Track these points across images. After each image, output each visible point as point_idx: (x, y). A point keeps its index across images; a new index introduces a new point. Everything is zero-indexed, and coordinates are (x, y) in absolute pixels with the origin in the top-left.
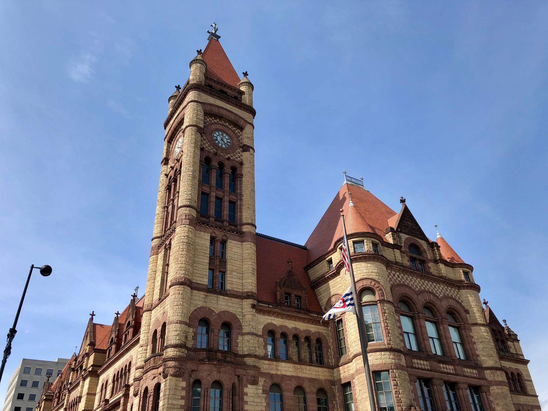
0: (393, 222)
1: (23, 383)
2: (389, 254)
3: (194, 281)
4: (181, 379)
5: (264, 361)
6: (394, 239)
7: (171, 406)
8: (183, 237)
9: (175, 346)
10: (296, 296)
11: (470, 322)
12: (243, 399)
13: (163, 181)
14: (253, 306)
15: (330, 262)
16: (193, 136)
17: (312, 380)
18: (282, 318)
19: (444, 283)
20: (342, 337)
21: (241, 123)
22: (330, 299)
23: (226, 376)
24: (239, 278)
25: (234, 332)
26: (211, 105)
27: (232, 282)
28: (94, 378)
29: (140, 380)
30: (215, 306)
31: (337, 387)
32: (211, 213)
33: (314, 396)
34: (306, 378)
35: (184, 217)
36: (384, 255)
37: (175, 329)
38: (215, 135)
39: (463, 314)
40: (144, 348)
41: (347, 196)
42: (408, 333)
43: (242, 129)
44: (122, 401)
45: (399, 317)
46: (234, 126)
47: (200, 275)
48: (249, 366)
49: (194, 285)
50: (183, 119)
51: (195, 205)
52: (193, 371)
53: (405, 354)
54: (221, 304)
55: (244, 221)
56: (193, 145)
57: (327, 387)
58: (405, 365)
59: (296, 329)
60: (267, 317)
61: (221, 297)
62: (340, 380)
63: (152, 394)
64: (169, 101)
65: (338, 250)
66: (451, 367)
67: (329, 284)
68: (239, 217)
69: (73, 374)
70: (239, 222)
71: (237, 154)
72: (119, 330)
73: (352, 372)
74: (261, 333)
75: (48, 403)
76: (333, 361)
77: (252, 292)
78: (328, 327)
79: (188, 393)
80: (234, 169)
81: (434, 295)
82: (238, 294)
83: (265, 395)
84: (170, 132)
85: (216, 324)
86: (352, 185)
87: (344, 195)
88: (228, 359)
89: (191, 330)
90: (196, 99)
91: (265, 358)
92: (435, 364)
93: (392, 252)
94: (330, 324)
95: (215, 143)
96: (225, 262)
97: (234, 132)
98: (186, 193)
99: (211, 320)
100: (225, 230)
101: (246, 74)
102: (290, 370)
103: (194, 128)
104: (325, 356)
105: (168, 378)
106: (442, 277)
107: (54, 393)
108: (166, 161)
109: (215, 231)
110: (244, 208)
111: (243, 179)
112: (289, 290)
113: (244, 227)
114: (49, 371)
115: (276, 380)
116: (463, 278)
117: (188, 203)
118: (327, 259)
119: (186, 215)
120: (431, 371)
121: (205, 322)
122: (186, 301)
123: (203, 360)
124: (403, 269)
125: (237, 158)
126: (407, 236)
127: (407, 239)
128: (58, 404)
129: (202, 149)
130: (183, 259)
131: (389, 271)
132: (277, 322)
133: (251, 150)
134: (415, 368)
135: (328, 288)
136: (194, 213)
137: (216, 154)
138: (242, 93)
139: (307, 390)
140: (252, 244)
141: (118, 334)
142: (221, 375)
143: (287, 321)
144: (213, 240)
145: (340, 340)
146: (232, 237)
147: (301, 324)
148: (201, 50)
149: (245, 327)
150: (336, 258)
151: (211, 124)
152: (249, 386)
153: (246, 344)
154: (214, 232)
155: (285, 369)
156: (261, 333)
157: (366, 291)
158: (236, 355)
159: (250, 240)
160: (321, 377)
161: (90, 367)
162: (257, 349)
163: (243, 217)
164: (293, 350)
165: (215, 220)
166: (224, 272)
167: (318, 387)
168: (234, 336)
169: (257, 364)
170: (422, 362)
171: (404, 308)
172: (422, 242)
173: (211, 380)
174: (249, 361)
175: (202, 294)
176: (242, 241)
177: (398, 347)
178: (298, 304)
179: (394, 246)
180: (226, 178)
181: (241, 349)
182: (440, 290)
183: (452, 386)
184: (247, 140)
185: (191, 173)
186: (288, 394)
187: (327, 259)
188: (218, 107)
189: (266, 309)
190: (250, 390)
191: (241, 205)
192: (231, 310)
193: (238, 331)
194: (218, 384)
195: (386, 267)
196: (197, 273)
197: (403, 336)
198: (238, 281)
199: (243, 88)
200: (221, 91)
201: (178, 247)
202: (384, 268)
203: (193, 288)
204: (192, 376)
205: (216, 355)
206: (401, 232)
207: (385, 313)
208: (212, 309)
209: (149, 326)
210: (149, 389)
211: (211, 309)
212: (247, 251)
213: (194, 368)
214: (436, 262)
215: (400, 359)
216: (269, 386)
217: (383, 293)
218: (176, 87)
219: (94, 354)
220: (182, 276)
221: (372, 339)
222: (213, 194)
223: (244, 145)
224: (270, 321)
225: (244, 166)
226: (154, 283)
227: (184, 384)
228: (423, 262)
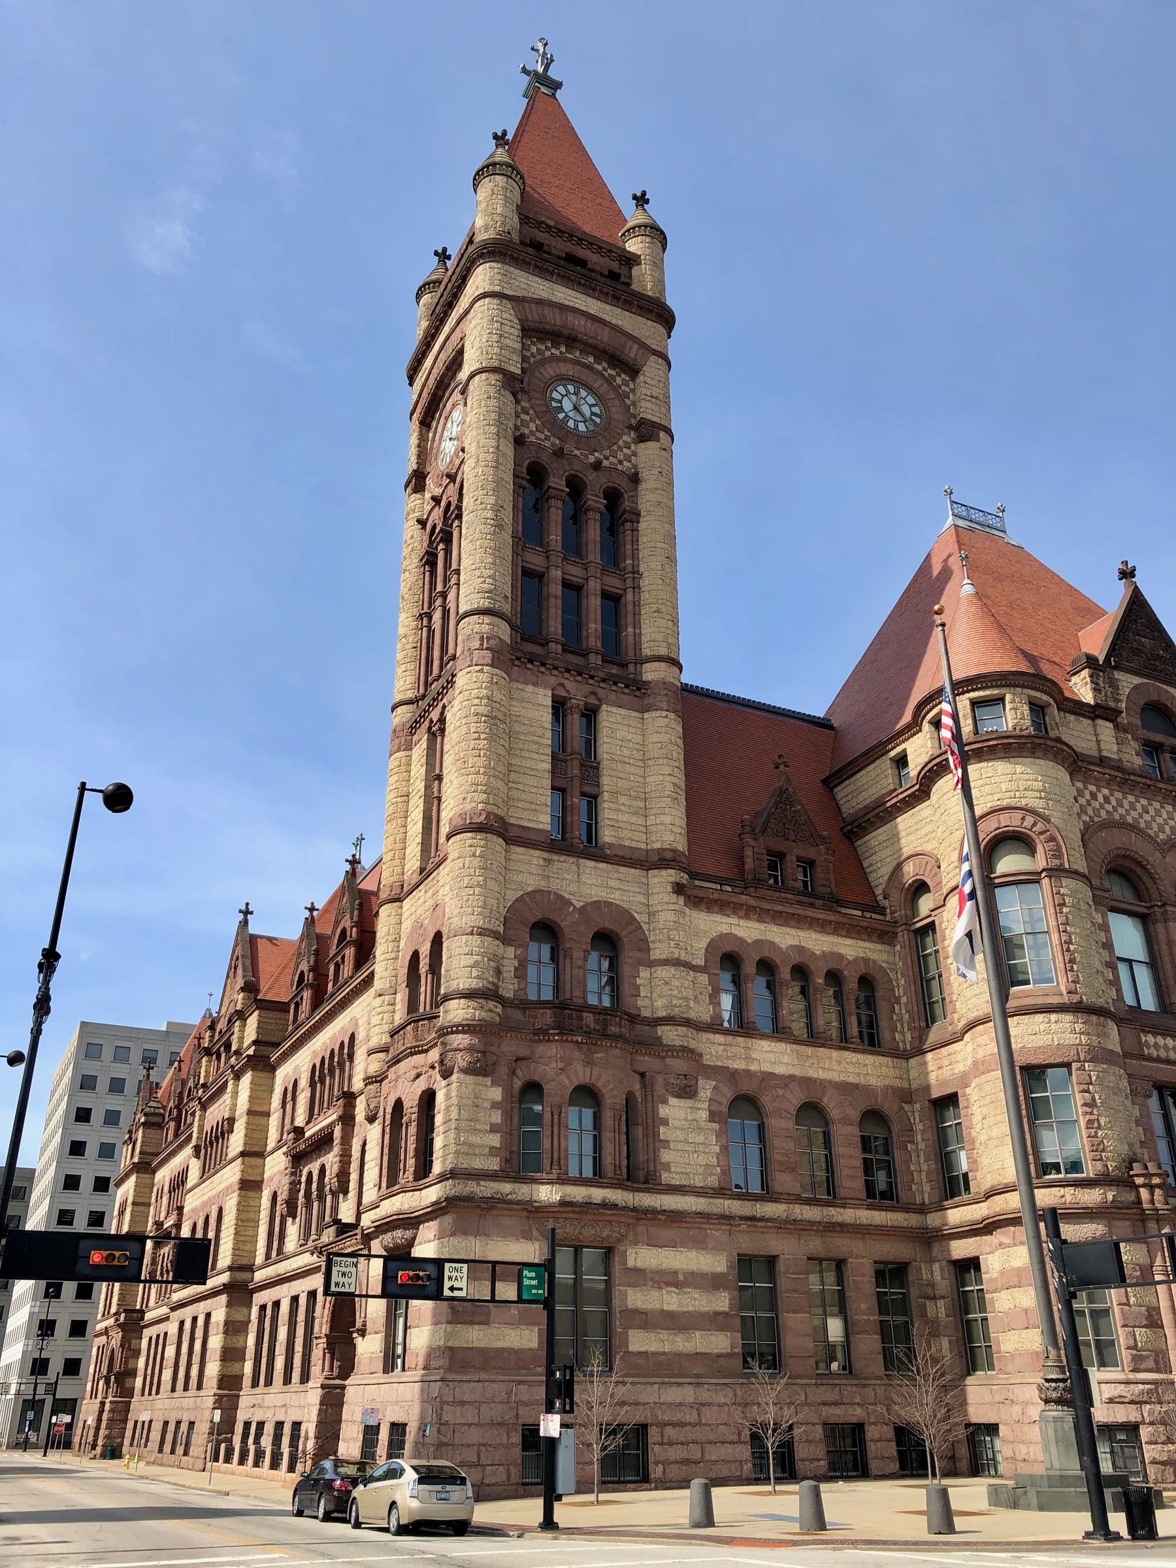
0: (1096, 640)
1: (86, 1083)
2: (1080, 735)
3: (513, 821)
4: (488, 1081)
5: (711, 1036)
6: (1096, 690)
7: (465, 1149)
8: (477, 701)
9: (469, 995)
12: (656, 1134)
13: (412, 541)
14: (679, 889)
15: (902, 761)
16: (493, 402)
17: (846, 1088)
18: (760, 920)
20: (933, 972)
21: (632, 355)
22: (899, 867)
23: (610, 1074)
24: (636, 813)
25: (628, 956)
26: (540, 302)
27: (618, 824)
28: (262, 1075)
29: (381, 1081)
30: (573, 888)
31: (917, 1106)
32: (552, 629)
33: (854, 1131)
34: (830, 1081)
35: (477, 644)
36: (1065, 738)
37: (466, 950)
38: (555, 395)
40: (387, 998)
41: (955, 563)
42: (1130, 962)
43: (633, 371)
45: (1104, 916)
46: (612, 366)
47: (527, 805)
48: (671, 1049)
49: (512, 833)
50: (460, 352)
51: (506, 608)
52: (518, 1059)
53: (1120, 1021)
54: (587, 884)
55: (647, 652)
56: (493, 429)
57: (889, 1107)
58: (1118, 1049)
59: (800, 949)
60: (718, 918)
62: (928, 1088)
63: (414, 1116)
64: (418, 297)
65: (926, 727)
67: (896, 825)
68: (631, 639)
69: (210, 1061)
70: (631, 653)
71: (620, 449)
72: (317, 950)
73: (960, 1068)
74: (700, 962)
75: (152, 1132)
76: (908, 1037)
77: (675, 851)
78: (894, 946)
79: (507, 1115)
80: (613, 497)
82: (636, 856)
83: (716, 1126)
84: (425, 394)
85: (577, 937)
86: (971, 530)
87: (946, 561)
88: (613, 1029)
89: (510, 952)
90: (497, 289)
91: (714, 1027)
93: (1090, 729)
94: (900, 938)
95: (555, 418)
96: (597, 768)
97: (610, 381)
98: (478, 573)
99: (563, 924)
100: (592, 677)
101: (641, 200)
102: (786, 1059)
103: (493, 378)
104: (883, 1023)
105: (454, 1077)
107: (164, 1108)
108: (418, 481)
109: (566, 682)
111: (642, 526)
112: (778, 845)
113: (647, 667)
114: (147, 1054)
115: (747, 1087)
117: (486, 604)
118: (892, 754)
119: (482, 639)
121: (546, 930)
122: (493, 874)
123: (545, 1032)
124: (1121, 777)
125: (621, 462)
126: (1137, 680)
127: (1136, 687)
128: (176, 1135)
129: (519, 441)
130: (481, 762)
131: (1080, 785)
132: (748, 930)
133: (662, 435)
134: (1150, 1059)
135: (895, 837)
136: (504, 632)
137: (559, 453)
138: (632, 260)
140: (672, 716)
141: (316, 961)
142: (596, 1072)
143: (775, 928)
144: (559, 707)
145: (928, 981)
146: (613, 697)
147: (815, 936)
148: (505, 133)
149: (658, 945)
150: (919, 749)
151: (544, 361)
152: (673, 1101)
153: (660, 991)
154: (562, 685)
155: (772, 1057)
156: (700, 962)
157: (1007, 845)
158: (634, 1019)
159: (665, 705)
160: (873, 1081)
161: (249, 1048)
162: (692, 1004)
163: (645, 639)
164: (792, 1007)
165: (563, 650)
166: (595, 797)
167: (864, 1105)
168: (626, 970)
169: (693, 1044)
171: (1120, 891)
173: (568, 1083)
174: (671, 1035)
176: (643, 710)
177: (1100, 1002)
178: (805, 883)
180: (591, 523)
181: (647, 1002)
184: (648, 405)
185: (490, 514)
186: (781, 1125)
187: (892, 754)
188: (562, 308)
189: (716, 896)
190: (674, 1110)
191: (637, 604)
192: (616, 898)
193: (638, 955)
194: (587, 1094)
195: (1071, 775)
196: (519, 800)
197: (1115, 969)
198: (633, 819)
199: (634, 246)
200: (571, 258)
201: (464, 729)
202: (1063, 775)
203: (509, 841)
204: (519, 1072)
205: (580, 1018)
206: (1116, 668)
207: (1063, 904)
208: (567, 896)
209: (397, 940)
210: (407, 1104)
211: (562, 898)
213: (523, 1052)
215: (1105, 1035)
216: (726, 1102)
217: (1059, 849)
218: (436, 253)
219: (256, 1013)
220: (480, 806)
221: (1021, 977)
222: (556, 574)
223: (643, 422)
224: (725, 929)
226: (405, 826)
227: (496, 1094)
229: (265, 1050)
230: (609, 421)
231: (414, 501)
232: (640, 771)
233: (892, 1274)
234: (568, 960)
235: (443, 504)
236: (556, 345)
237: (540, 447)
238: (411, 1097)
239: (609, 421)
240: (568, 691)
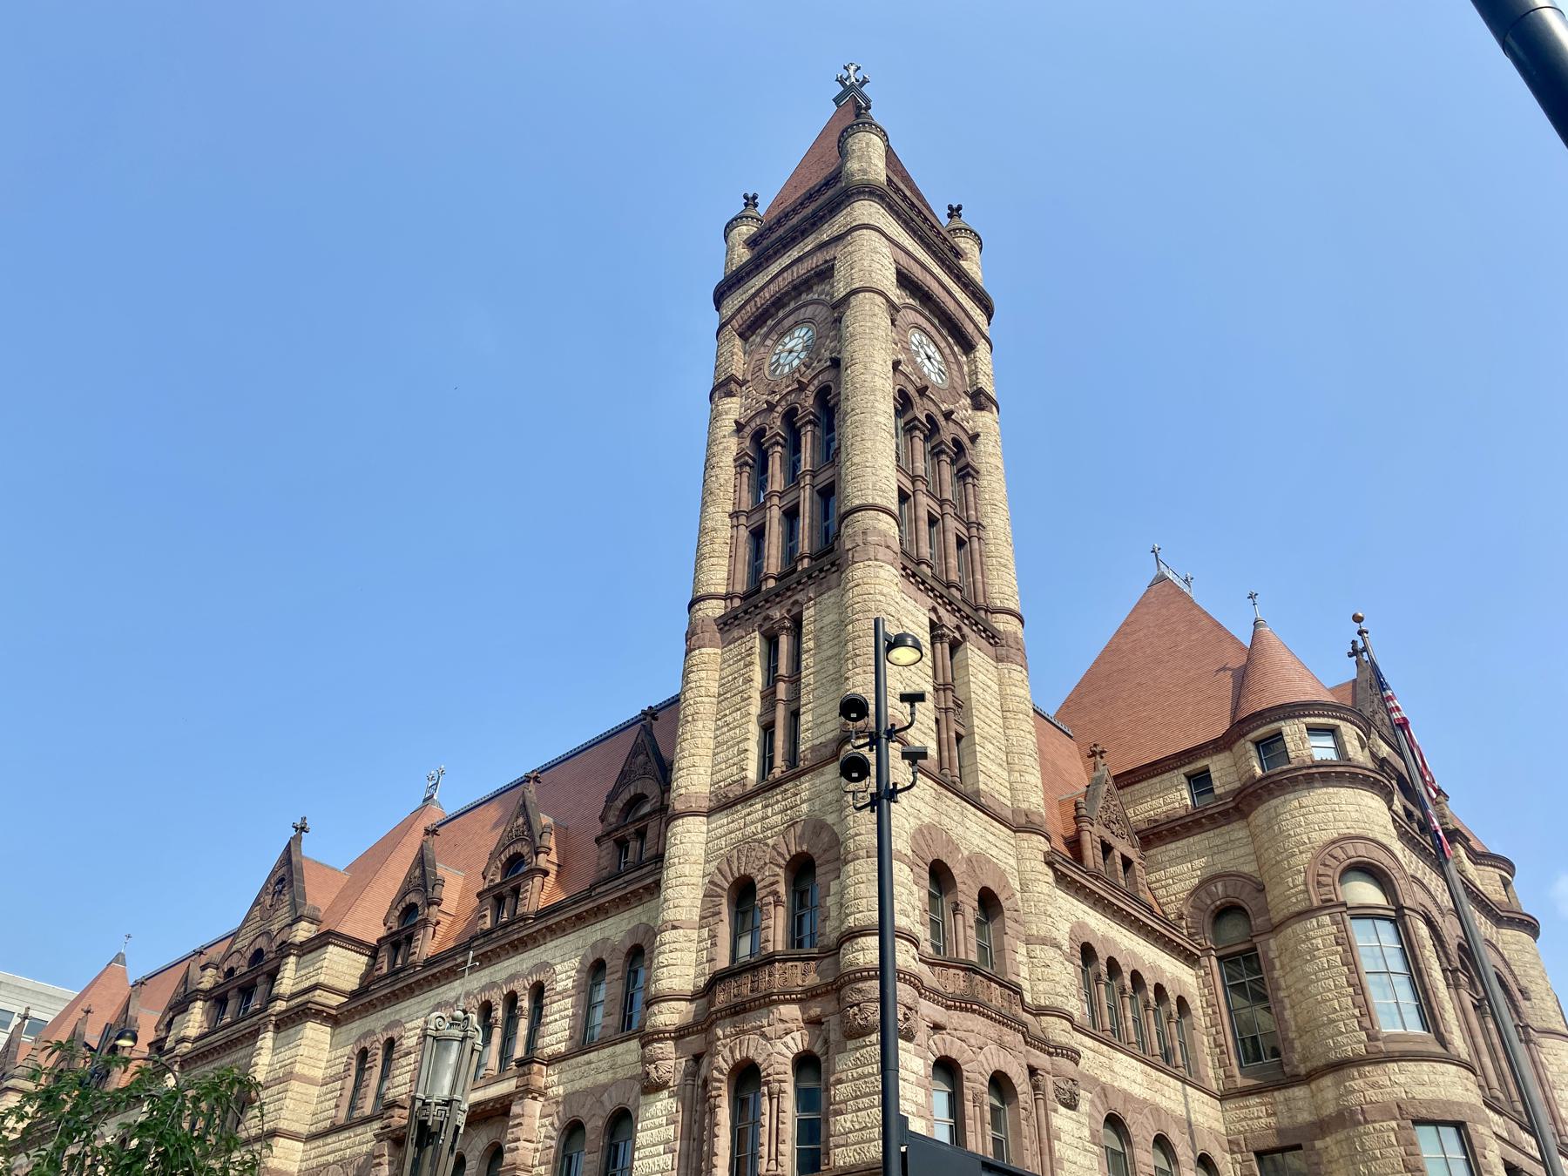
10: (1123, 857)
59: (1133, 955)
64: (729, 227)
68: (979, 585)
70: (981, 600)
101: (954, 212)
109: (941, 611)
115: (1119, 1107)
129: (896, 365)
152: (1062, 1109)
174: (1058, 1030)
198: (1000, 771)
218: (746, 197)
232: (1000, 721)
234: (959, 917)
240: (939, 618)
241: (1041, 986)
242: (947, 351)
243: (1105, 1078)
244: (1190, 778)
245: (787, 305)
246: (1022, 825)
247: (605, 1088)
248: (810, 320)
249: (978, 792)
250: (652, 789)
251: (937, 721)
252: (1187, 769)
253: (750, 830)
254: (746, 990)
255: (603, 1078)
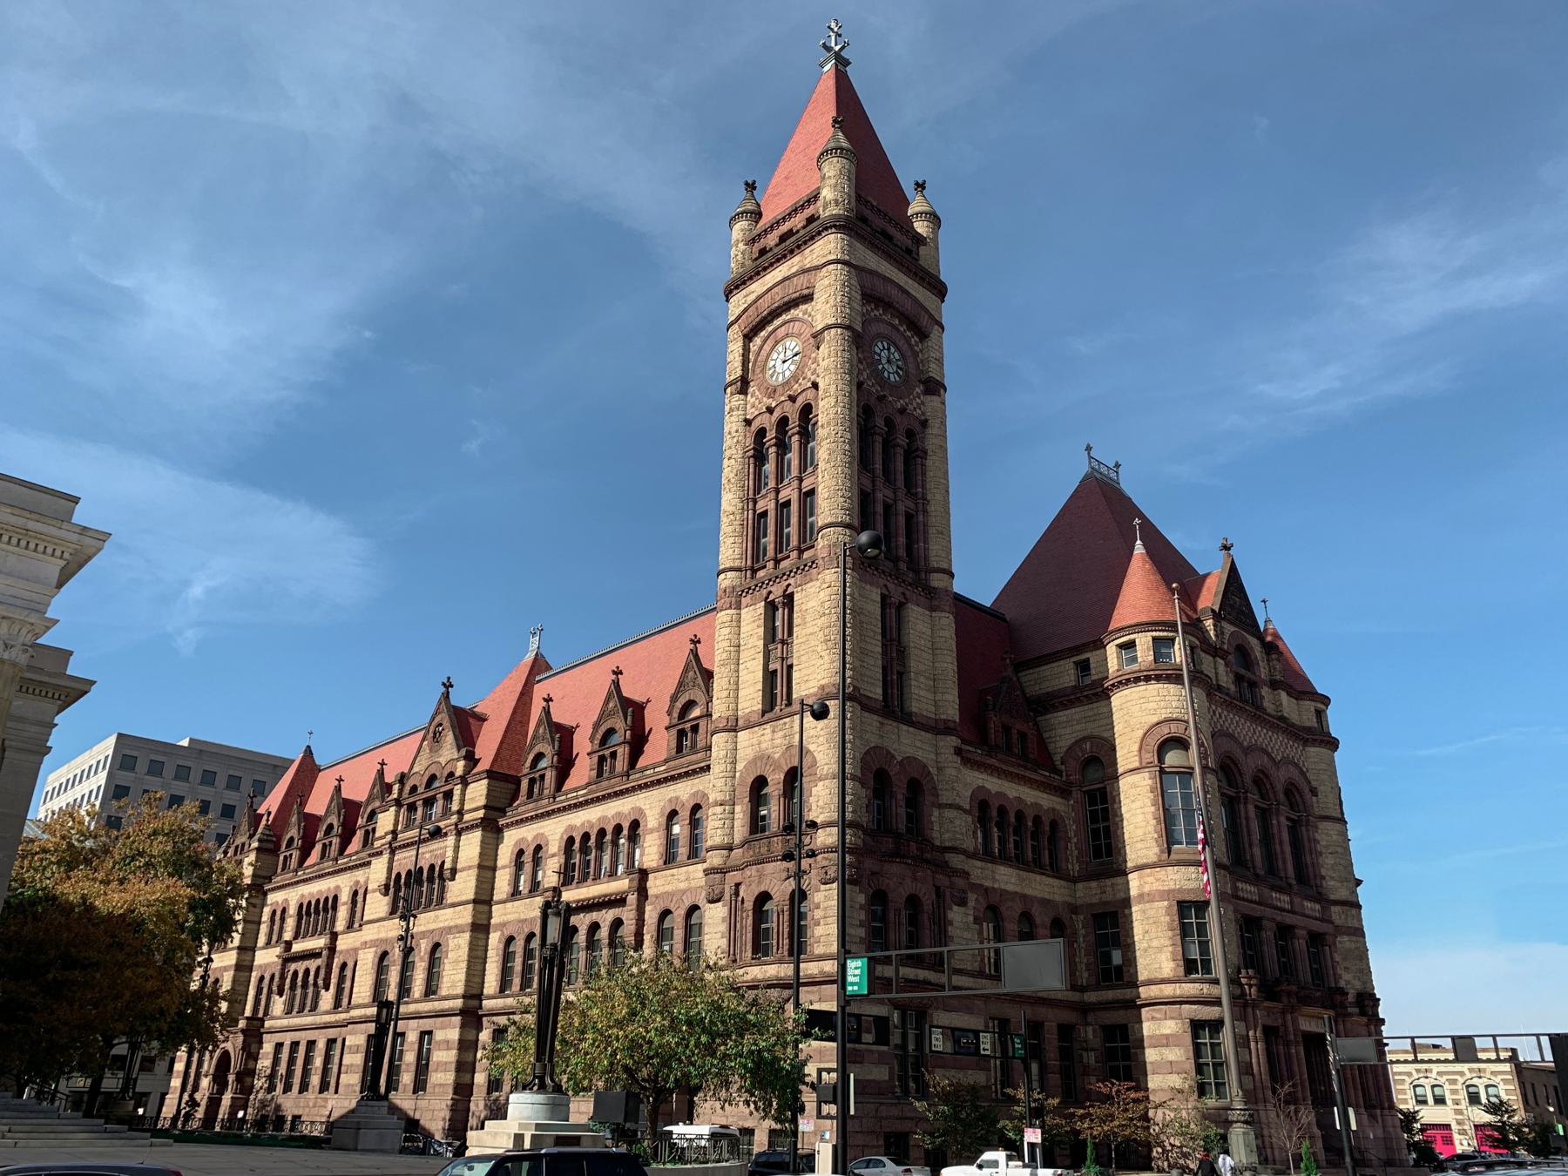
10: (1019, 732)
11: (1317, 811)
14: (958, 752)
16: (847, 355)
17: (1045, 902)
19: (1285, 731)
25: (928, 799)
26: (872, 273)
27: (920, 699)
39: (1308, 795)
43: (923, 336)
44: (632, 899)
49: (864, 701)
54: (908, 744)
60: (977, 774)
61: (905, 727)
66: (1287, 898)
69: (397, 813)
75: (269, 858)
80: (910, 434)
81: (1269, 755)
89: (863, 792)
91: (972, 856)
92: (1266, 891)
97: (907, 340)
101: (920, 186)
106: (1282, 719)
108: (743, 385)
110: (932, 531)
111: (929, 463)
116: (1313, 722)
120: (1259, 903)
122: (859, 732)
126: (1233, 629)
129: (860, 385)
132: (993, 784)
137: (881, 399)
138: (919, 240)
139: (1038, 920)
152: (955, 908)
155: (1006, 878)
158: (934, 848)
160: (1057, 898)
163: (932, 553)
169: (966, 868)
170: (1248, 887)
172: (1254, 642)
173: (904, 892)
174: (956, 861)
175: (873, 720)
176: (932, 609)
179: (1215, 651)
182: (1278, 745)
183: (1285, 932)
190: (956, 915)
192: (920, 755)
199: (921, 227)
209: (734, 762)
212: (942, 633)
213: (876, 868)
214: (1274, 685)
219: (485, 782)
222: (879, 496)
225: (929, 431)
228: (1253, 685)
229: (493, 814)
230: (907, 373)
231: (737, 400)
233: (1066, 1031)
235: (777, 414)
236: (877, 308)
237: (869, 392)
238: (781, 890)
239: (907, 373)
241: (946, 836)
242: (905, 348)
243: (988, 884)
244: (1076, 663)
245: (780, 315)
246: (939, 728)
247: (684, 892)
248: (799, 336)
249: (910, 714)
250: (698, 695)
251: (884, 668)
252: (1075, 659)
253: (764, 746)
254: (764, 850)
255: (682, 886)
